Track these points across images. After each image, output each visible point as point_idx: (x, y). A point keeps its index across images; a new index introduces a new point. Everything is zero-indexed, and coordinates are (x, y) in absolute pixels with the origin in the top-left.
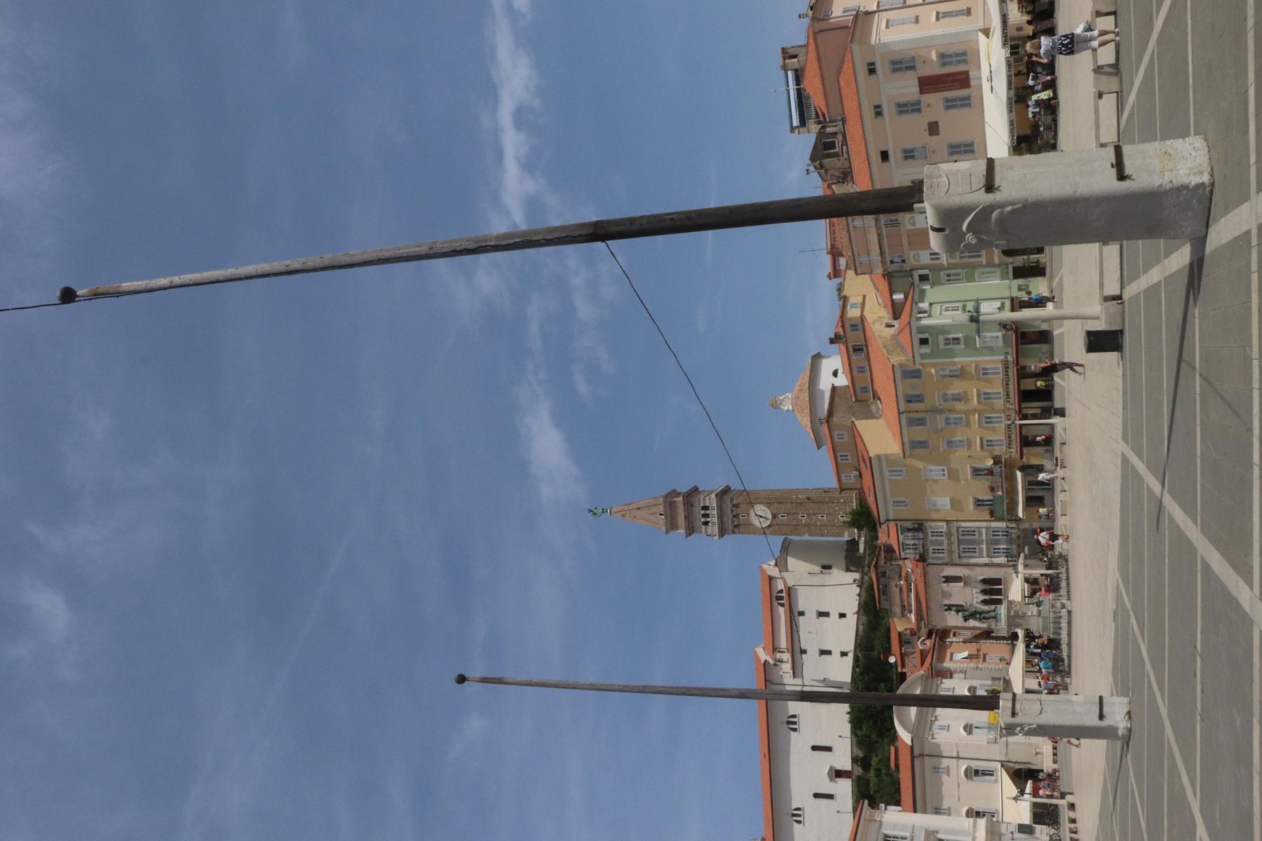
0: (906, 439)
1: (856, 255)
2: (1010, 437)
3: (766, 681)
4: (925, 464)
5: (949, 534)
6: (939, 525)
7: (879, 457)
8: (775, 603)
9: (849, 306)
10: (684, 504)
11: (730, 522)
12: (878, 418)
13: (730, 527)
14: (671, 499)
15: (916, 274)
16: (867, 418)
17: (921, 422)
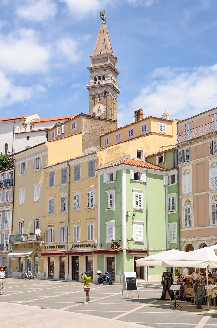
0: (54, 169)
1: (192, 120)
2: (53, 247)
3: (15, 119)
4: (41, 184)
5: (6, 204)
6: (11, 198)
7: (46, 150)
8: (57, 122)
9: (160, 123)
10: (106, 65)
11: (96, 93)
12: (83, 151)
13: (93, 93)
14: (109, 57)
15: (175, 172)
16: (84, 143)
17: (64, 180)
